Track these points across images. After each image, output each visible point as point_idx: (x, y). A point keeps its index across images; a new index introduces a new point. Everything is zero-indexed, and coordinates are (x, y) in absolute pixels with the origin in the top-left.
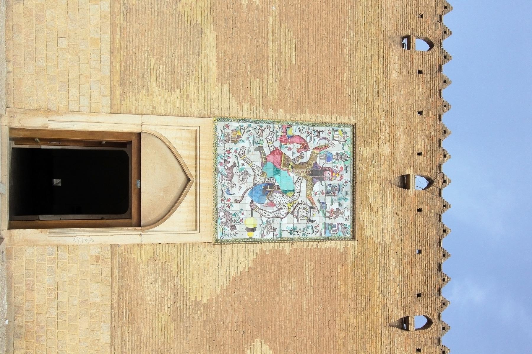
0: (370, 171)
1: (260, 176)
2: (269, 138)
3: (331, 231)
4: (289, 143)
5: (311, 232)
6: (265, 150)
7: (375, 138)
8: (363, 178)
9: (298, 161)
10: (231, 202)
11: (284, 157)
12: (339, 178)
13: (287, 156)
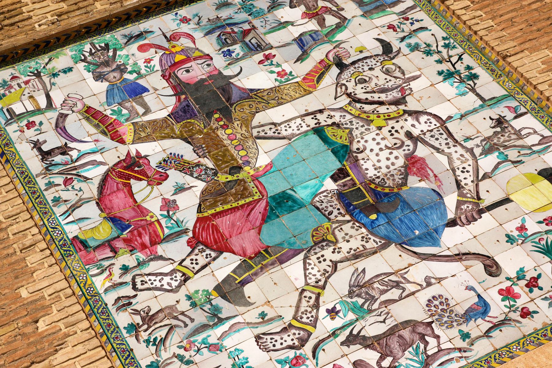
4: (148, 218)
6: (221, 275)
9: (198, 165)
10: (509, 283)
11: (213, 205)
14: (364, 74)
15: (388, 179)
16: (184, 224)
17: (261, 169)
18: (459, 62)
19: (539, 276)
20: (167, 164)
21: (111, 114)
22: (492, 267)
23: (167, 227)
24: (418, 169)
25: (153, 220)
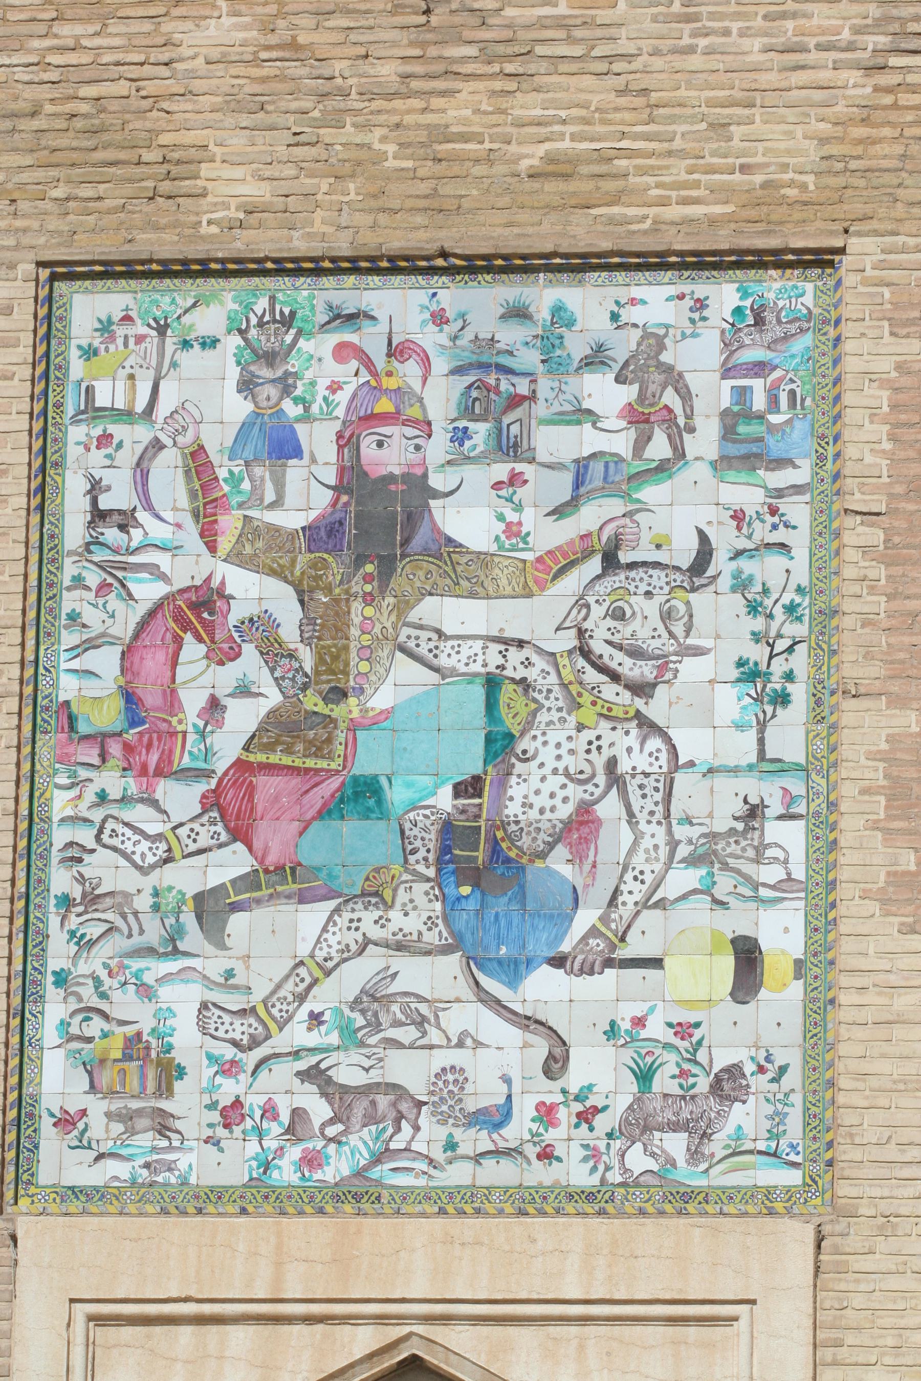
0: (363, 155)
1: (389, 907)
2: (139, 849)
3: (774, 419)
4: (174, 721)
5: (775, 562)
6: (214, 879)
7: (138, 124)
8: (409, 203)
9: (292, 656)
11: (269, 748)
12: (411, 370)
13: (262, 729)
14: (633, 600)
15: (529, 833)
16: (214, 759)
17: (371, 714)
18: (785, 655)
19: (606, 1108)
20: (250, 630)
21: (225, 480)
22: (556, 1061)
23: (190, 753)
24: (580, 838)
25: (180, 728)
